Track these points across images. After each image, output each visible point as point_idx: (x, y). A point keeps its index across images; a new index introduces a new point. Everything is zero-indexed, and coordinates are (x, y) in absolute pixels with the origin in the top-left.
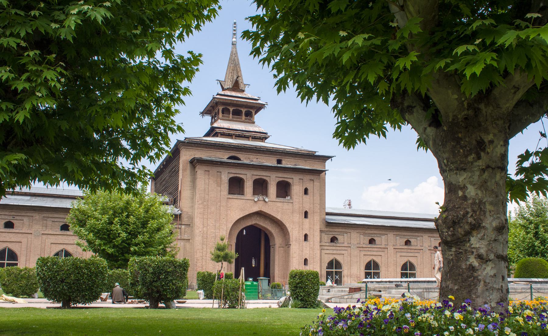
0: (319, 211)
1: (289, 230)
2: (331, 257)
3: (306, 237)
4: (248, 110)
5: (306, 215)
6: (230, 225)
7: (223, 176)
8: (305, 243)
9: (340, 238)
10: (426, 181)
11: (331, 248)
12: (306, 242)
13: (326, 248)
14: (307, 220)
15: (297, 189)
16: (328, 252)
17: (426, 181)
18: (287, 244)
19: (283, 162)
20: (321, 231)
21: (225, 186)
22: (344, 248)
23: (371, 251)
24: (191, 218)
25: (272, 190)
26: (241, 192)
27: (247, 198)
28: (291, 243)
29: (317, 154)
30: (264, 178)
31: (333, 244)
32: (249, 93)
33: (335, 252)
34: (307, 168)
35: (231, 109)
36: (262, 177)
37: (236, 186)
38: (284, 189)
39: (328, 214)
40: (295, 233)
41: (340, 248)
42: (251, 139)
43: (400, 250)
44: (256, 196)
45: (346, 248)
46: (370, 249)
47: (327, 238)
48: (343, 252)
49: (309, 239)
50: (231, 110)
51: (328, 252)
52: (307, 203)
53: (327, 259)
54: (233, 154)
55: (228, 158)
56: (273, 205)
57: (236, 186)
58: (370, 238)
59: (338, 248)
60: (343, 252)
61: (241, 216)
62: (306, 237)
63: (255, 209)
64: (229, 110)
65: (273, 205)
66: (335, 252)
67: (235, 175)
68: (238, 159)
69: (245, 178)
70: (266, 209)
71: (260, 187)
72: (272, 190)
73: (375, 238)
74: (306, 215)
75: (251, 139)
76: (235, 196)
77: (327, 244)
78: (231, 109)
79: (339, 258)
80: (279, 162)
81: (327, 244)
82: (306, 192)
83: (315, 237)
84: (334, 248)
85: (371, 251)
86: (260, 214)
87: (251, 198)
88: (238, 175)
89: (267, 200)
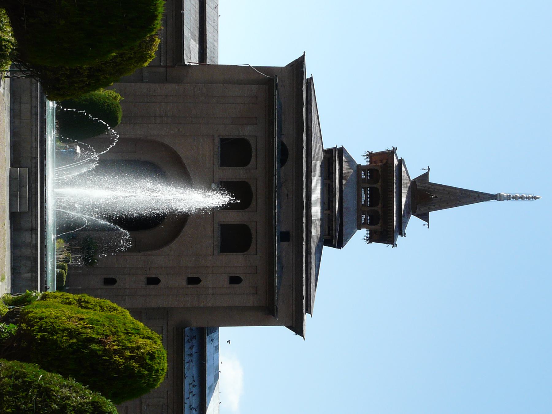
0: (202, 305)
1: (166, 249)
3: (153, 281)
5: (194, 281)
8: (143, 279)
12: (144, 280)
14: (185, 283)
15: (236, 262)
19: (285, 244)
26: (225, 161)
28: (142, 253)
30: (254, 202)
35: (378, 186)
36: (254, 197)
49: (151, 286)
50: (376, 186)
54: (290, 153)
62: (153, 281)
67: (253, 150)
68: (283, 162)
69: (249, 166)
74: (194, 281)
76: (218, 150)
80: (285, 237)
82: (235, 280)
88: (254, 154)
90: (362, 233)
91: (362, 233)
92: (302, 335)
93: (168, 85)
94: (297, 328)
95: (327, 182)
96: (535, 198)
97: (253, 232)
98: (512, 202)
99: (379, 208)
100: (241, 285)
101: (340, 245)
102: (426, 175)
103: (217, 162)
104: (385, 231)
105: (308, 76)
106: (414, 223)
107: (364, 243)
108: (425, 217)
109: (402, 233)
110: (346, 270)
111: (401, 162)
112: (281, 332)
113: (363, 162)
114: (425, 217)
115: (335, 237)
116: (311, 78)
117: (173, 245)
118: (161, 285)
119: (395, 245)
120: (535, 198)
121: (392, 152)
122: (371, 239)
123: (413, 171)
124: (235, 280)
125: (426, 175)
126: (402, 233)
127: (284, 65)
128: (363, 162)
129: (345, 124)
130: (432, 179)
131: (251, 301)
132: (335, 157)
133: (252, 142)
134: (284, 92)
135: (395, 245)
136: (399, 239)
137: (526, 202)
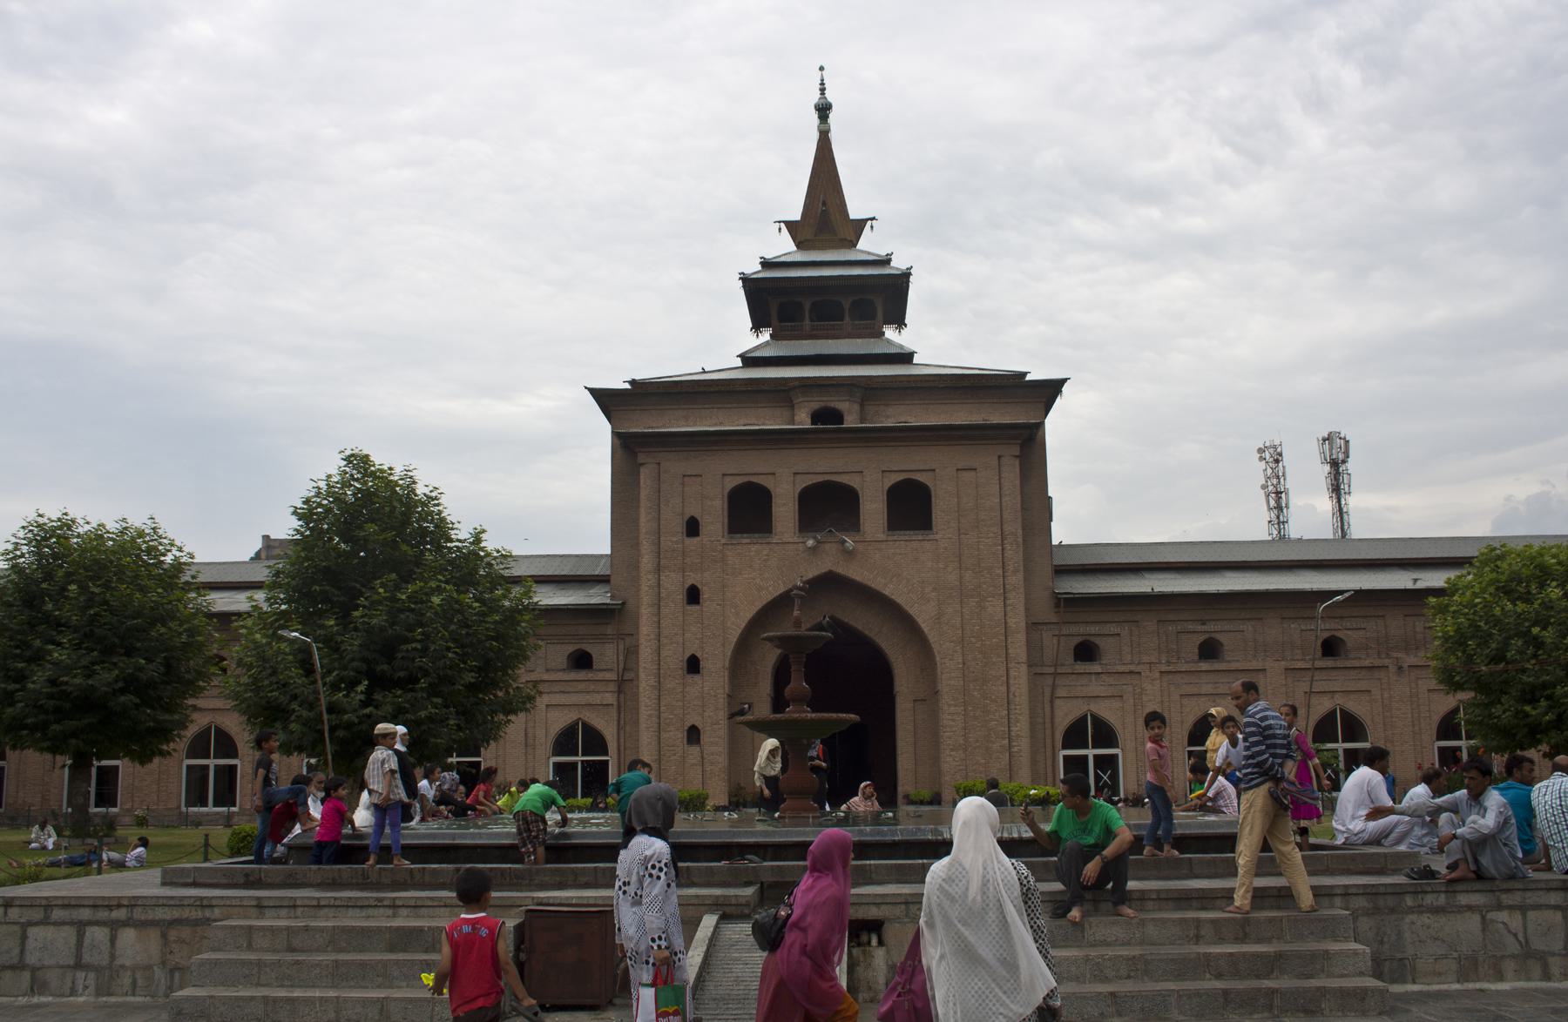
4: (886, 294)
20: (1033, 626)
32: (869, 244)
39: (1062, 571)
53: (1066, 714)
57: (749, 510)
67: (746, 479)
70: (840, 570)
71: (828, 506)
78: (847, 305)
86: (829, 583)
90: (890, 333)
92: (1063, 381)
94: (1050, 390)
102: (790, 225)
106: (869, 244)
108: (860, 225)
111: (766, 264)
114: (860, 225)
122: (899, 321)
123: (783, 246)
126: (886, 261)
134: (647, 422)
136: (899, 264)
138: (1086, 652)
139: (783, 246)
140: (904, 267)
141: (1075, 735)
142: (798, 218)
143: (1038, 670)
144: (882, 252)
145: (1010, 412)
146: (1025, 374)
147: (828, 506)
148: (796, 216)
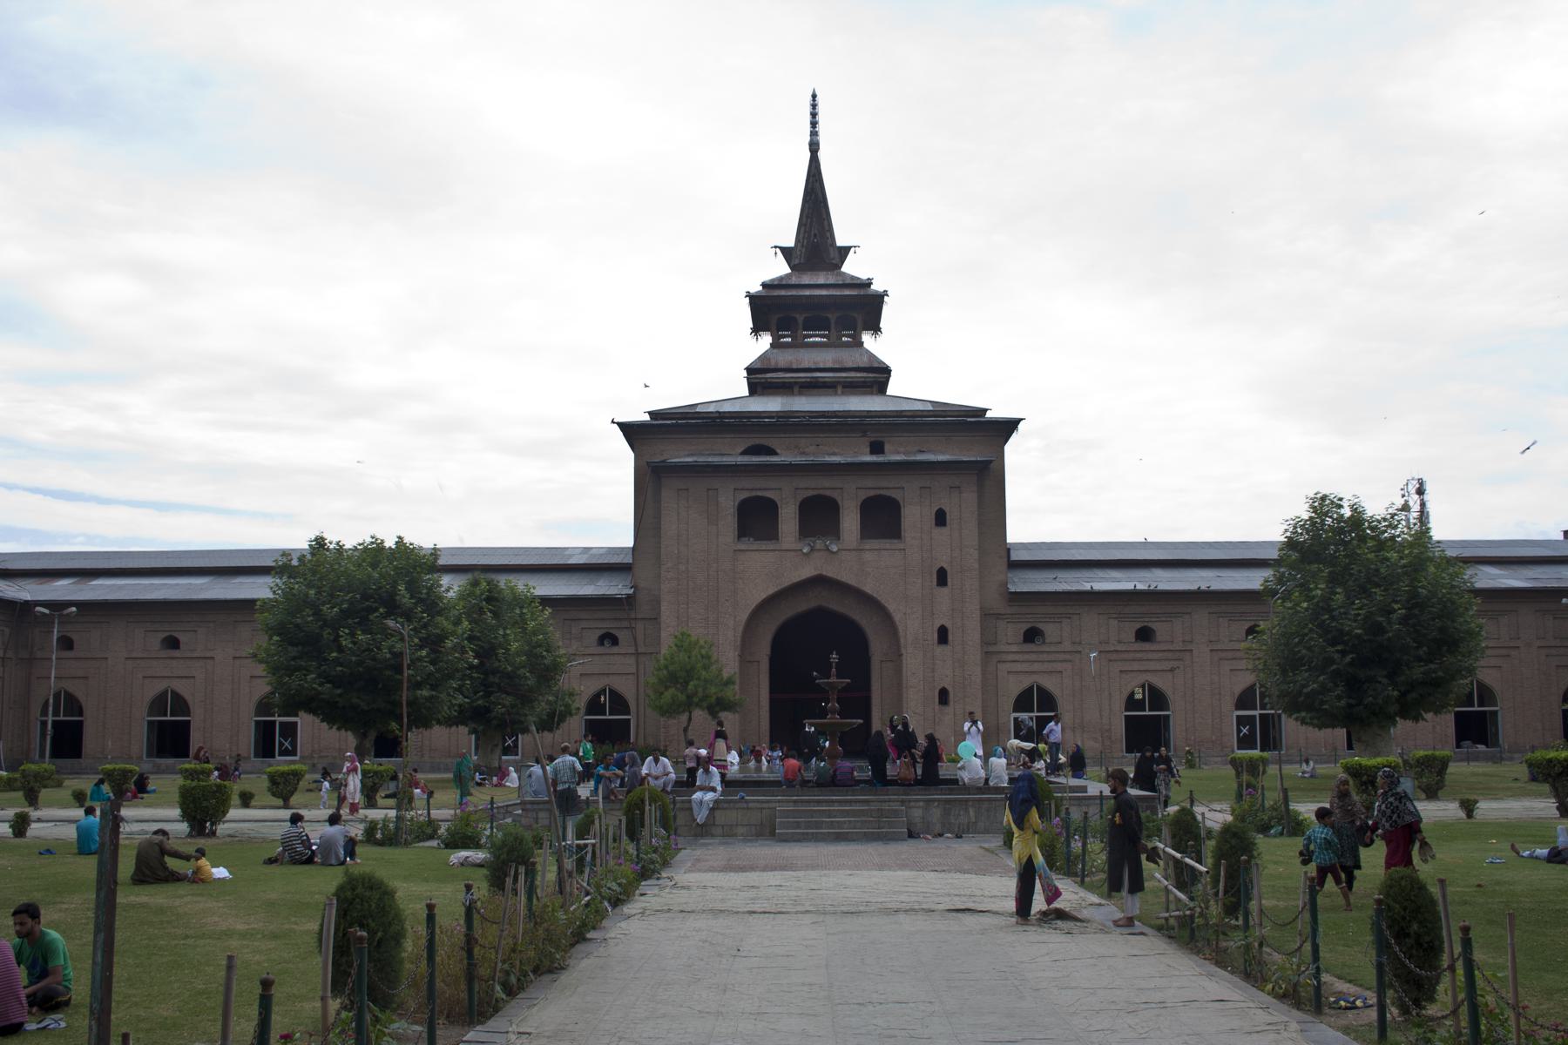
0: (976, 566)
1: (897, 617)
2: (1026, 682)
3: (943, 635)
5: (942, 577)
6: (744, 616)
7: (722, 499)
8: (940, 649)
9: (1050, 630)
10: (320, 543)
11: (1027, 657)
12: (943, 647)
13: (1010, 657)
14: (945, 590)
15: (915, 515)
16: (1019, 667)
17: (320, 543)
18: (896, 655)
19: (887, 447)
20: (987, 616)
21: (729, 522)
22: (1062, 657)
23: (1141, 660)
24: (657, 602)
25: (850, 521)
27: (785, 546)
29: (989, 414)
30: (828, 493)
31: (1031, 647)
33: (1036, 667)
34: (941, 458)
35: (800, 318)
37: (756, 519)
38: (882, 518)
40: (913, 625)
41: (1052, 657)
42: (840, 390)
43: (1230, 655)
44: (808, 540)
45: (1068, 657)
46: (1139, 655)
47: (1010, 633)
48: (1059, 666)
51: (1019, 667)
52: (944, 547)
53: (1014, 687)
54: (758, 442)
55: (744, 453)
56: (853, 559)
57: (756, 519)
58: (1138, 626)
59: (1045, 657)
60: (1059, 666)
61: (771, 591)
62: (943, 635)
63: (807, 572)
64: (795, 320)
65: (853, 559)
66: (1036, 667)
67: (754, 494)
70: (830, 572)
71: (819, 516)
72: (850, 521)
73: (1153, 626)
74: (942, 577)
75: (840, 390)
77: (1014, 648)
79: (1049, 684)
80: (877, 448)
81: (1014, 648)
82: (940, 519)
83: (969, 634)
84: (1033, 657)
85: (1141, 660)
86: (820, 582)
87: (793, 546)
88: (760, 493)
89: (834, 548)
90: (867, 339)
91: (867, 339)
93: (664, 618)
94: (1009, 426)
95: (796, 389)
96: (814, 96)
97: (872, 493)
98: (821, 128)
99: (832, 317)
100: (947, 510)
101: (885, 371)
102: (786, 252)
103: (771, 545)
104: (865, 307)
105: (647, 418)
107: (881, 338)
109: (868, 283)
110: (922, 359)
111: (764, 285)
112: (1015, 452)
113: (766, 341)
115: (878, 376)
116: (650, 413)
117: (891, 607)
118: (948, 625)
119: (885, 293)
120: (814, 96)
121: (754, 299)
122: (875, 328)
123: (780, 268)
124: (940, 519)
125: (786, 252)
126: (868, 283)
127: (632, 455)
128: (766, 341)
129: (714, 361)
130: (790, 242)
131: (970, 497)
132: (760, 378)
133: (744, 495)
135: (885, 293)
136: (877, 287)
137: (821, 109)
138: (1032, 635)
139: (780, 268)
140: (881, 290)
141: (1023, 703)
142: (792, 244)
143: (991, 649)
144: (864, 276)
145: (972, 445)
146: (985, 410)
147: (819, 516)
148: (790, 242)
